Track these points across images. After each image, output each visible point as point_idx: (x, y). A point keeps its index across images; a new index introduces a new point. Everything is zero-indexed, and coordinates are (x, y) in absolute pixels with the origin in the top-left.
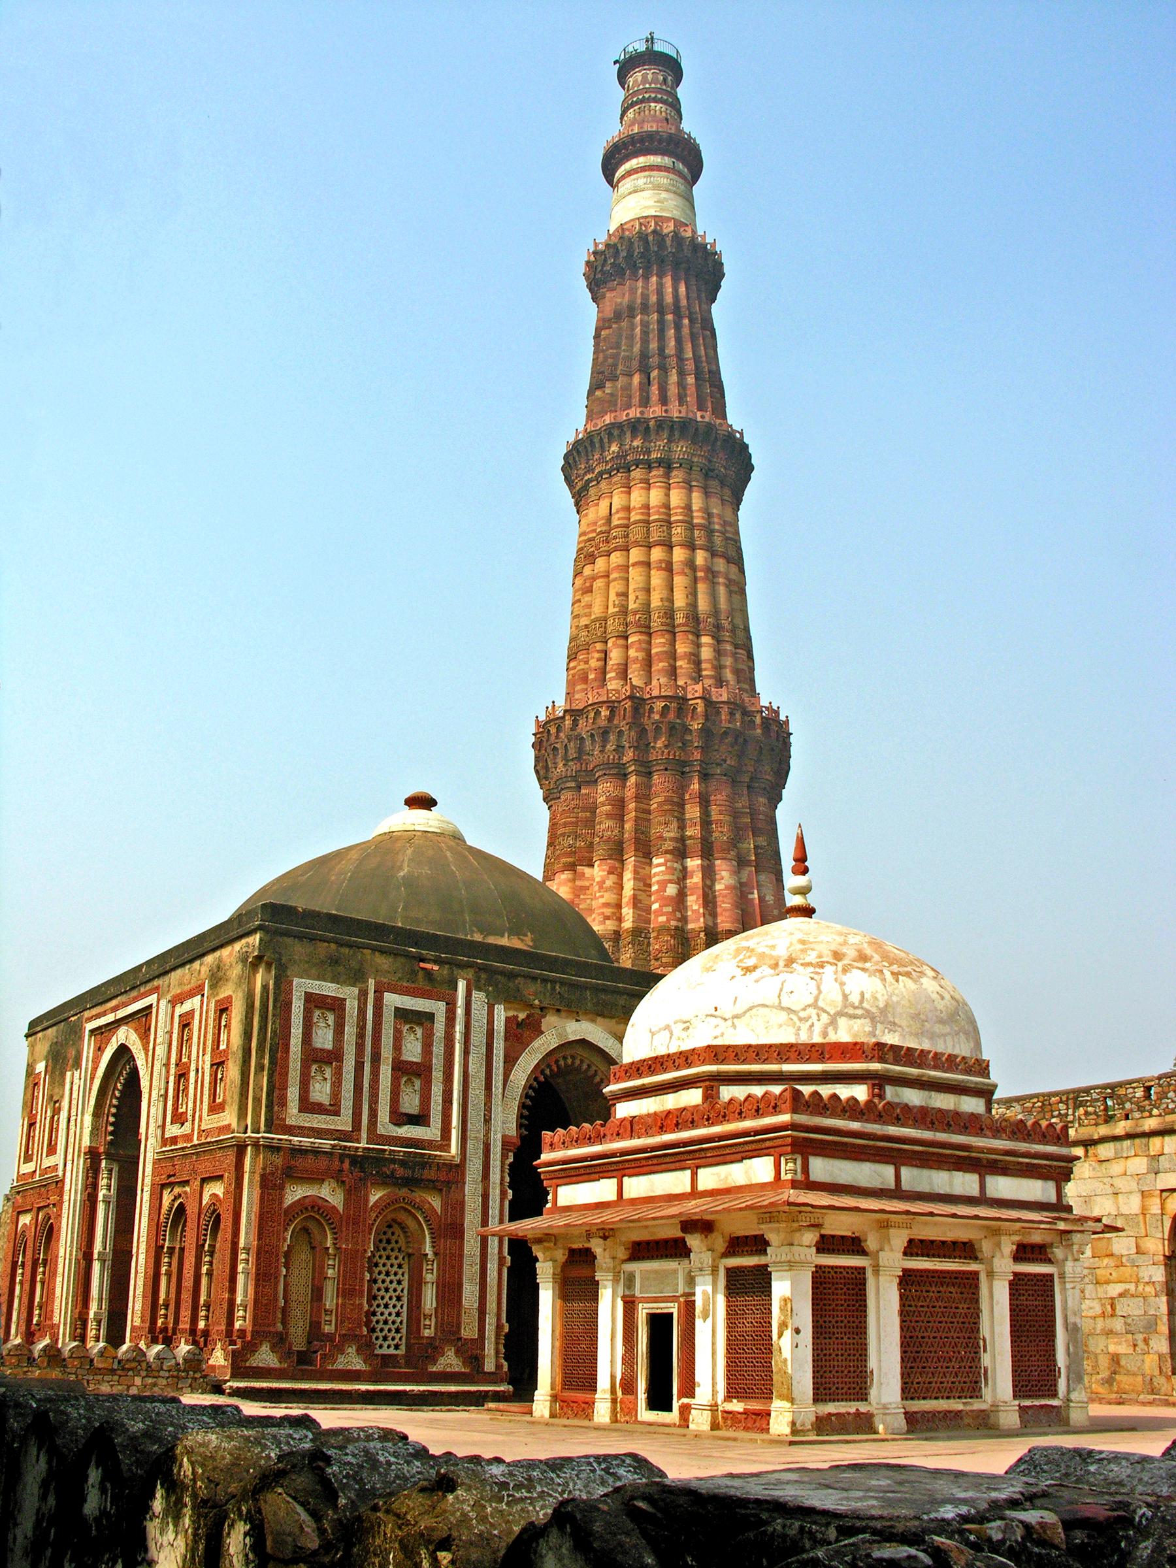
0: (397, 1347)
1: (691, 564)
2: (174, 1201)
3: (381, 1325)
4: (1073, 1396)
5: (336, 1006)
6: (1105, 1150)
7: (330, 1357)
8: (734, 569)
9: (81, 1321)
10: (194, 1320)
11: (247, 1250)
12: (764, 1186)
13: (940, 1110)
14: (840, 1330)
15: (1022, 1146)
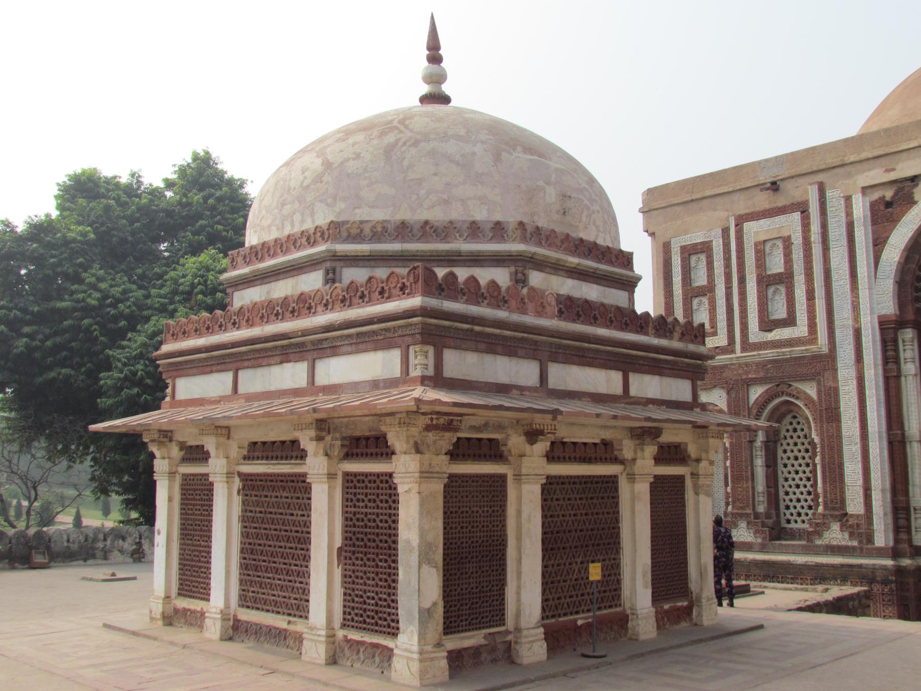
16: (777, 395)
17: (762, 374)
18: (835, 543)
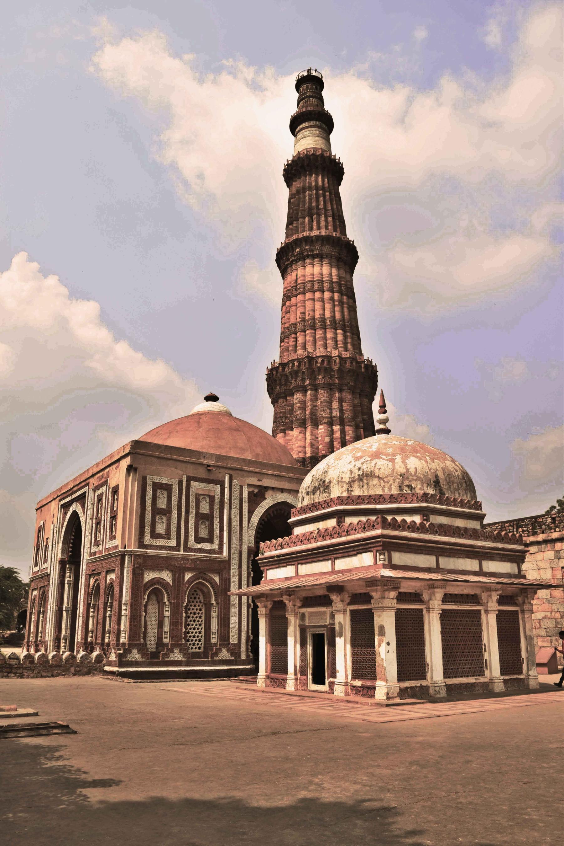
0: (199, 648)
1: (332, 299)
2: (95, 582)
3: (192, 638)
4: (530, 673)
5: (168, 488)
7: (167, 655)
8: (351, 301)
9: (57, 639)
10: (103, 638)
11: (126, 605)
12: (369, 567)
13: (457, 527)
14: (410, 642)
15: (500, 545)
16: (199, 579)
17: (193, 566)
18: (224, 659)
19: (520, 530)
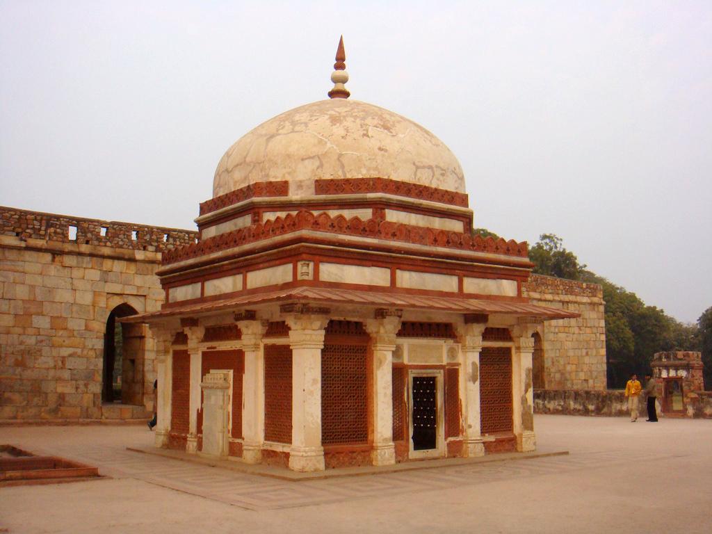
6: (69, 260)
19: (52, 230)
